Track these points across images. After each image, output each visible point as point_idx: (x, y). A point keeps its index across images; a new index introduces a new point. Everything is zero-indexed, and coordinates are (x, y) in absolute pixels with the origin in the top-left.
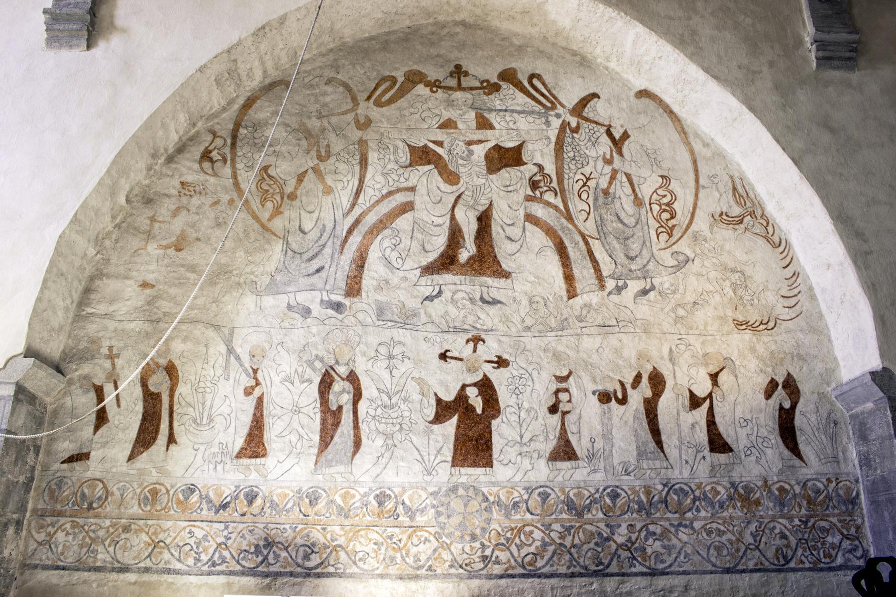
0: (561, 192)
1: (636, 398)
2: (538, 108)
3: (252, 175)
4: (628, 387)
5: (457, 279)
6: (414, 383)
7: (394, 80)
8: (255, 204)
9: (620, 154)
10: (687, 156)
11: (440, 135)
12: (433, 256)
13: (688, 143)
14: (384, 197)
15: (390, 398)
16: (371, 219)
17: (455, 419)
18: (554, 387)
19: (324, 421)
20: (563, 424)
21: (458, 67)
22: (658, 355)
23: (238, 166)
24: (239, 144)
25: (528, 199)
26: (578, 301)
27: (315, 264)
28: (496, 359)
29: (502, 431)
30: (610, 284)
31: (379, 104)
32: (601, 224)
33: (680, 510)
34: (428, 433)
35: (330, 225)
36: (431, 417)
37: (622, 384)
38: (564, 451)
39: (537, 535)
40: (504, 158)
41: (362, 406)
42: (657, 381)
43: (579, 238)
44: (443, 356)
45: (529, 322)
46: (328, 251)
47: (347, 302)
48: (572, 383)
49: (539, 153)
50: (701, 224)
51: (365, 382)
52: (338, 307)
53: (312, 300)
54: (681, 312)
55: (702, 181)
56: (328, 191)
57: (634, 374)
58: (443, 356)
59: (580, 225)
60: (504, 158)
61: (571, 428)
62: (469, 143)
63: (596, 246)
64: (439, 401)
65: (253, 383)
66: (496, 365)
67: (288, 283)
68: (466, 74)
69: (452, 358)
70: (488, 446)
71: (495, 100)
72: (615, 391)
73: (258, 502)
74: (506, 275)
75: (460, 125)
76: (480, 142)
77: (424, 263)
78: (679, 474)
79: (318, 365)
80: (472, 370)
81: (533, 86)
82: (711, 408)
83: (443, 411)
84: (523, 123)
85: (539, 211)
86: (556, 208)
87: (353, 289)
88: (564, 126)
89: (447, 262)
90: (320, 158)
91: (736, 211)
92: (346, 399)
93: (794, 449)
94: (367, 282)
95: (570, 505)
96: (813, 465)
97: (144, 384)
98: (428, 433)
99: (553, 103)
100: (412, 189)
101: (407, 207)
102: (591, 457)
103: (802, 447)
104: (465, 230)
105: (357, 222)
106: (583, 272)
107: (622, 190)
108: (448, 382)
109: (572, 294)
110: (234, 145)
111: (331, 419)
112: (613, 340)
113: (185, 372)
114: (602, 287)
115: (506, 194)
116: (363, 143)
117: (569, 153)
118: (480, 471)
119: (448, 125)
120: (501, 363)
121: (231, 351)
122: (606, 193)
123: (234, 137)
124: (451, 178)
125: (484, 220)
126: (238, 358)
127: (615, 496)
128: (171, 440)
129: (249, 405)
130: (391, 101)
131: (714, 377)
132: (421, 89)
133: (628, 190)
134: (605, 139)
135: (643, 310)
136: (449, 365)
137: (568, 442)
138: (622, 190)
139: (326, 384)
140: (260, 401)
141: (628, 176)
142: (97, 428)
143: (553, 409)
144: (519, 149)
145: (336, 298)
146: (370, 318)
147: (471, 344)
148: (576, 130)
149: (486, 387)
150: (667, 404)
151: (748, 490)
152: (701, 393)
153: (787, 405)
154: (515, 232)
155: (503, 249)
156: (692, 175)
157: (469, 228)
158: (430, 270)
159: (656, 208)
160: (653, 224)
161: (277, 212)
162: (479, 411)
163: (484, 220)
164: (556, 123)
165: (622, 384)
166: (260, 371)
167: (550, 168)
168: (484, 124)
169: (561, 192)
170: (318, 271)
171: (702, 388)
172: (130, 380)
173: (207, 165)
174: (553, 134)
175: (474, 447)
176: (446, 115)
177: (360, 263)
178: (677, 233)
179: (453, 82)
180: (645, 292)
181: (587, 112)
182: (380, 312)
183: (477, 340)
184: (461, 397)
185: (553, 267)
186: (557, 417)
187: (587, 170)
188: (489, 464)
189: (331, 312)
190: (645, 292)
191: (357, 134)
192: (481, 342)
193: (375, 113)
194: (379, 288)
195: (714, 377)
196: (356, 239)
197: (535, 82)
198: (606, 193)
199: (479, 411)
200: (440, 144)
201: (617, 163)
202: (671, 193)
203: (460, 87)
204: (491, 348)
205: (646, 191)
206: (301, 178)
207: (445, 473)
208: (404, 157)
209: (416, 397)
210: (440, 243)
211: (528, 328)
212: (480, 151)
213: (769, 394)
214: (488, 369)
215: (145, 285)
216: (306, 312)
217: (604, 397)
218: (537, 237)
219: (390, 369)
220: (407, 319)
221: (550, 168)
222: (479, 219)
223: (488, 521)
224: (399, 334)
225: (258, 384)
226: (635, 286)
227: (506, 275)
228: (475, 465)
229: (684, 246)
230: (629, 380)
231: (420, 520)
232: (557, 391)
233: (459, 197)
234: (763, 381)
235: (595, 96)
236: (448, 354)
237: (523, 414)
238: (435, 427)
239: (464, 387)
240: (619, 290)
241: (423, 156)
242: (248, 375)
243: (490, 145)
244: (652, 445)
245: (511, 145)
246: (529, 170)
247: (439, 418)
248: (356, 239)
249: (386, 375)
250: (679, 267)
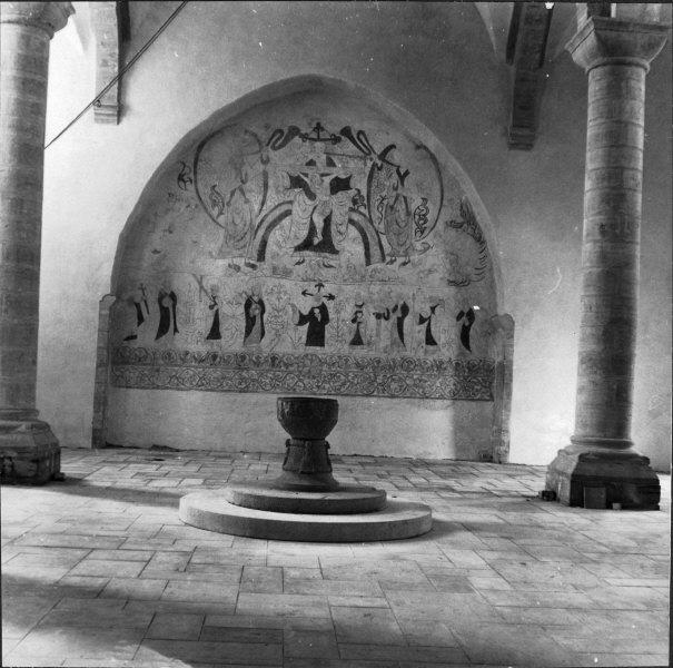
0: (369, 207)
1: (394, 318)
2: (361, 154)
3: (208, 191)
5: (311, 253)
7: (281, 131)
8: (210, 209)
9: (403, 184)
10: (438, 187)
11: (307, 170)
12: (300, 242)
13: (441, 180)
14: (276, 207)
16: (270, 219)
18: (356, 309)
19: (247, 322)
21: (318, 124)
22: (407, 291)
23: (199, 185)
24: (199, 171)
25: (352, 210)
26: (372, 267)
27: (242, 243)
29: (329, 330)
30: (388, 259)
31: (274, 148)
32: (388, 226)
33: (408, 370)
34: (296, 330)
35: (248, 223)
38: (357, 341)
39: (342, 377)
40: (340, 185)
41: (265, 316)
42: (405, 310)
43: (374, 233)
44: (304, 293)
45: (346, 277)
46: (248, 237)
47: (258, 264)
48: (364, 309)
49: (360, 184)
50: (440, 226)
51: (266, 303)
52: (253, 266)
53: (241, 262)
54: (422, 275)
55: (444, 202)
56: (247, 201)
58: (304, 293)
59: (376, 225)
60: (340, 185)
61: (362, 330)
62: (322, 175)
63: (383, 238)
64: (301, 315)
67: (229, 253)
68: (323, 129)
70: (323, 337)
71: (337, 149)
73: (218, 359)
74: (336, 252)
75: (318, 164)
76: (327, 175)
77: (296, 244)
78: (409, 354)
79: (244, 295)
81: (358, 138)
82: (429, 324)
83: (303, 319)
84: (352, 164)
85: (356, 217)
86: (365, 216)
87: (261, 256)
88: (374, 165)
89: (307, 245)
90: (242, 181)
91: (460, 220)
92: (257, 312)
93: (468, 347)
94: (268, 255)
95: (358, 365)
96: (474, 356)
97: (160, 301)
98: (296, 330)
99: (371, 150)
100: (291, 202)
101: (288, 213)
102: (369, 344)
103: (471, 345)
104: (317, 225)
105: (262, 221)
106: (375, 250)
107: (401, 207)
108: (306, 305)
109: (368, 262)
110: (195, 173)
111: (250, 321)
112: (386, 288)
113: (181, 299)
114: (383, 259)
115: (340, 205)
116: (265, 174)
117: (374, 183)
118: (318, 348)
119: (311, 163)
120: (331, 297)
121: (202, 287)
122: (392, 207)
123: (195, 167)
124: (312, 196)
125: (327, 221)
126: (205, 291)
127: (379, 362)
128: (176, 330)
129: (211, 313)
130: (281, 146)
131: (433, 309)
132: (297, 139)
133: (404, 207)
134: (395, 176)
135: (405, 273)
137: (360, 338)
138: (401, 207)
139: (248, 305)
141: (405, 198)
142: (139, 324)
143: (354, 321)
144: (348, 180)
145: (252, 262)
146: (268, 272)
148: (380, 169)
149: (323, 308)
150: (407, 321)
151: (442, 363)
152: (425, 316)
153: (467, 324)
154: (343, 229)
155: (336, 239)
156: (439, 198)
157: (319, 224)
158: (299, 248)
159: (417, 217)
160: (414, 226)
161: (221, 213)
163: (327, 221)
164: (370, 164)
167: (364, 193)
168: (330, 163)
169: (369, 207)
170: (245, 246)
171: (426, 313)
172: (152, 298)
173: (182, 184)
174: (367, 170)
175: (316, 337)
176: (310, 157)
177: (264, 244)
178: (426, 232)
179: (314, 136)
180: (404, 264)
181: (388, 157)
182: (275, 270)
183: (320, 285)
184: (312, 312)
185: (360, 249)
186: (355, 325)
187: (384, 194)
188: (323, 345)
189: (251, 269)
190: (404, 264)
191: (261, 167)
193: (272, 154)
194: (273, 258)
195: (433, 309)
196: (261, 233)
197: (361, 137)
198: (392, 207)
200: (306, 175)
201: (399, 192)
202: (427, 208)
203: (319, 139)
204: (328, 288)
205: (413, 207)
206: (232, 194)
207: (302, 350)
208: (287, 182)
210: (304, 233)
211: (345, 281)
212: (327, 180)
213: (458, 318)
214: (325, 300)
215: (155, 252)
216: (238, 268)
217: (378, 316)
218: (353, 232)
220: (287, 273)
221: (364, 193)
222: (325, 221)
223: (321, 370)
224: (283, 282)
225: (216, 304)
226: (400, 260)
227: (336, 252)
228: (317, 345)
229: (429, 239)
231: (291, 369)
232: (356, 313)
233: (315, 208)
234: (457, 312)
235: (393, 147)
239: (313, 308)
240: (392, 262)
241: (297, 182)
243: (333, 176)
244: (399, 340)
245: (344, 177)
246: (352, 193)
247: (301, 323)
248: (261, 233)
250: (425, 250)
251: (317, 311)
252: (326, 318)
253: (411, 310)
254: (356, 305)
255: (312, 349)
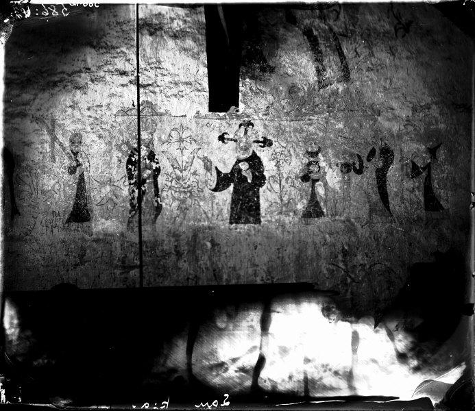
4: (364, 159)
6: (199, 160)
15: (181, 172)
17: (231, 188)
18: (306, 161)
20: (313, 190)
28: (262, 140)
36: (214, 186)
37: (359, 157)
44: (222, 138)
57: (370, 148)
58: (222, 138)
64: (219, 173)
65: (74, 164)
66: (262, 145)
69: (228, 139)
72: (354, 164)
80: (246, 149)
83: (223, 181)
129: (72, 180)
136: (226, 145)
137: (317, 204)
140: (82, 176)
143: (305, 178)
147: (243, 128)
149: (254, 161)
150: (393, 172)
162: (249, 181)
165: (359, 157)
166: (79, 155)
184: (236, 170)
192: (251, 126)
199: (249, 181)
209: (201, 171)
214: (255, 148)
219: (182, 150)
225: (79, 165)
230: (365, 156)
232: (309, 164)
236: (226, 136)
237: (283, 182)
238: (216, 194)
239: (239, 161)
242: (70, 158)
244: (381, 204)
249: (176, 153)
251: (244, 166)
252: (259, 179)
253: (397, 156)
254: (308, 152)
255: (243, 228)
